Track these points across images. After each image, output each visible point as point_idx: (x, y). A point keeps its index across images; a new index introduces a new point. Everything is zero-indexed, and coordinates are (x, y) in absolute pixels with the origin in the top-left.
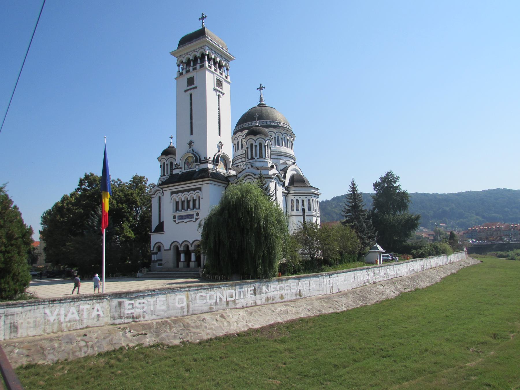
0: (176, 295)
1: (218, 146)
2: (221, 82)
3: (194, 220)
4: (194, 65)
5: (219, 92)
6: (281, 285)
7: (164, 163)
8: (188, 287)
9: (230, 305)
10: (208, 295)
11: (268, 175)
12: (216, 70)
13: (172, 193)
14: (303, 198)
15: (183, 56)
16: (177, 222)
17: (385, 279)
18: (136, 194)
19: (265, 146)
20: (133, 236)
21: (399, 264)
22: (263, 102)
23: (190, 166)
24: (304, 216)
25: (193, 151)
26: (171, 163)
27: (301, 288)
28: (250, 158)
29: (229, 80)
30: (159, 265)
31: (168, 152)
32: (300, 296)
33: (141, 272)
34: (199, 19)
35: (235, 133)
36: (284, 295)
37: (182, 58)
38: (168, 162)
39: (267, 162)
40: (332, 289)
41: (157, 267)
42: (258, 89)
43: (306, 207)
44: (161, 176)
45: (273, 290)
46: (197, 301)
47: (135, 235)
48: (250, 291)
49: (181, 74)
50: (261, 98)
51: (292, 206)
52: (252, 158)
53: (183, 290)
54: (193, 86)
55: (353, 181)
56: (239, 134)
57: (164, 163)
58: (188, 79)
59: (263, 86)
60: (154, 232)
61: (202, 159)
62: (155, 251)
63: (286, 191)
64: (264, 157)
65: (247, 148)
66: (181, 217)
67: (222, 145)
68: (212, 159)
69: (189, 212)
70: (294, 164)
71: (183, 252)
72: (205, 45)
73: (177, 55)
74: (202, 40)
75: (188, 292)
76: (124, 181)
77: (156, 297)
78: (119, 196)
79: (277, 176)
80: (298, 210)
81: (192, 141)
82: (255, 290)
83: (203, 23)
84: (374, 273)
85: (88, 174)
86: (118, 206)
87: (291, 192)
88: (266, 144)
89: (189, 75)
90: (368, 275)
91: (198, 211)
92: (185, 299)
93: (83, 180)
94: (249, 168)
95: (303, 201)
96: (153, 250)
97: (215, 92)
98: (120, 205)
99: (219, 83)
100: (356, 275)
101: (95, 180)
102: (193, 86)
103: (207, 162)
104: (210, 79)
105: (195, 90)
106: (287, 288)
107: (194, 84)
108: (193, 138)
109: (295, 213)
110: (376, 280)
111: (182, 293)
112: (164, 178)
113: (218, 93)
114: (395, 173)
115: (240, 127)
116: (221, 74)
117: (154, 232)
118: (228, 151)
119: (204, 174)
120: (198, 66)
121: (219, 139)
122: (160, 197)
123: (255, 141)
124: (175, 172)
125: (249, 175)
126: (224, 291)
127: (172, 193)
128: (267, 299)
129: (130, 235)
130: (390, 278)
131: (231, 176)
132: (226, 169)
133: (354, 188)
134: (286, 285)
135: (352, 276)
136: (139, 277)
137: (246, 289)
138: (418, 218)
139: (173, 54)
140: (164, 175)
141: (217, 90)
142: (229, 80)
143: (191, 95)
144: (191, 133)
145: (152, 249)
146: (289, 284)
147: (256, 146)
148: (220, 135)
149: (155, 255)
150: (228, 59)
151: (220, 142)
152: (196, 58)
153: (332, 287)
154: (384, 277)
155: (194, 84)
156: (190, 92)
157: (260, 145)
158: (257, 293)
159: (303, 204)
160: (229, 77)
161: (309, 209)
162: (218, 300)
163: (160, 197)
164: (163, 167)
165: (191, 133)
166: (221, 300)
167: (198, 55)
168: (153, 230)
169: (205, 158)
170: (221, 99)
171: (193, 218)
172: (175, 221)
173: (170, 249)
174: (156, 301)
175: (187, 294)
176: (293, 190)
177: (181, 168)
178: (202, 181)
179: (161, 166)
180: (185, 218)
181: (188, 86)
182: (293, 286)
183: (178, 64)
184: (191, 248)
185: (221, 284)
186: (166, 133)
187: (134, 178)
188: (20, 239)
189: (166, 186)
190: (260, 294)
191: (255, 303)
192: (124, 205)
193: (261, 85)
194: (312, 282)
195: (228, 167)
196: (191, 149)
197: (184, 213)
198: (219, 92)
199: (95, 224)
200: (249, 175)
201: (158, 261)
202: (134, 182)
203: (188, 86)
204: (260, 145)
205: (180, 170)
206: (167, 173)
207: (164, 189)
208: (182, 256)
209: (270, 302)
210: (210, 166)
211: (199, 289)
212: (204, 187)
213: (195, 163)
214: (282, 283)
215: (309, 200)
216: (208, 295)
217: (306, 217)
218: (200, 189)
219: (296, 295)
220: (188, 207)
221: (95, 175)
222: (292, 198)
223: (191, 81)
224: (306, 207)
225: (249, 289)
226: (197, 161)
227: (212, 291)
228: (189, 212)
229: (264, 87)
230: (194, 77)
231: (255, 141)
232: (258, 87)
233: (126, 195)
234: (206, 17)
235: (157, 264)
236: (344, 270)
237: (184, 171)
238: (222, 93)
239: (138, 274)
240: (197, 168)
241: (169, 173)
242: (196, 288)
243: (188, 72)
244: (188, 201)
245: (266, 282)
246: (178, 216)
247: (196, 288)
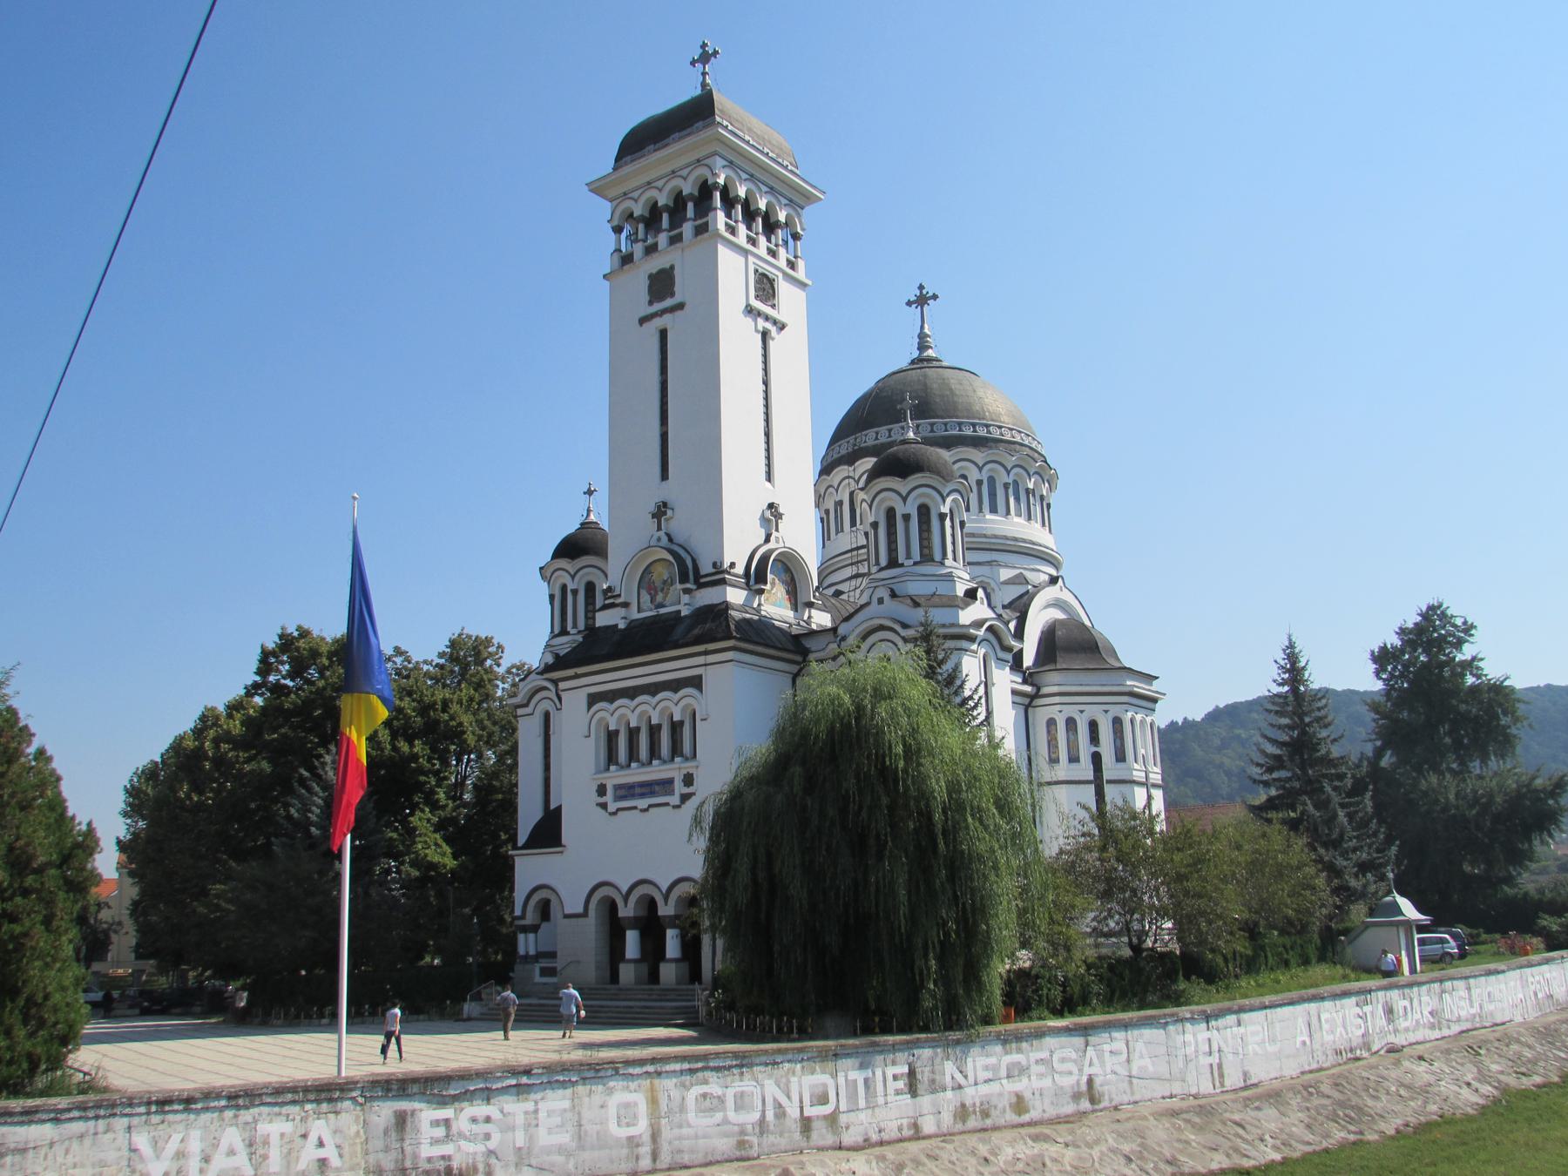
0: (611, 1091)
1: (765, 521)
2: (771, 282)
3: (675, 800)
4: (673, 226)
5: (767, 318)
6: (1015, 1057)
7: (564, 587)
8: (653, 1060)
9: (814, 1135)
10: (730, 1092)
11: (957, 625)
13: (593, 699)
15: (635, 195)
16: (612, 807)
17: (1437, 1034)
18: (460, 702)
19: (942, 517)
20: (450, 863)
21: (1489, 973)
22: (930, 353)
23: (659, 598)
24: (1098, 783)
25: (670, 540)
26: (590, 588)
27: (1092, 1071)
28: (883, 562)
29: (801, 274)
30: (547, 972)
31: (579, 546)
32: (1093, 1100)
33: (478, 998)
34: (693, 63)
35: (826, 469)
36: (1027, 1095)
37: (628, 204)
38: (578, 584)
39: (950, 575)
40: (1221, 1076)
41: (538, 979)
42: (909, 303)
44: (554, 636)
45: (983, 1075)
46: (691, 1116)
47: (455, 856)
48: (895, 1078)
49: (627, 259)
50: (922, 337)
51: (1052, 743)
52: (893, 563)
53: (637, 1070)
54: (668, 303)
55: (1291, 646)
56: (842, 471)
57: (564, 588)
58: (651, 276)
59: (930, 290)
60: (526, 846)
61: (706, 568)
62: (528, 921)
63: (1028, 689)
64: (938, 557)
65: (875, 525)
66: (627, 791)
67: (778, 516)
68: (739, 569)
69: (657, 771)
70: (1053, 580)
71: (635, 923)
72: (715, 154)
73: (613, 193)
74: (704, 135)
75: (657, 1081)
76: (416, 657)
77: (533, 1096)
78: (400, 710)
79: (990, 629)
80: (1074, 759)
81: (665, 504)
82: (912, 1074)
83: (704, 74)
84: (1389, 1011)
85: (292, 630)
86: (395, 749)
87: (1045, 690)
88: (945, 509)
89: (656, 263)
90: (1363, 1017)
91: (688, 767)
92: (643, 1108)
93: (273, 653)
94: (881, 601)
95: (1093, 726)
96: (523, 917)
97: (749, 321)
98: (404, 747)
99: (765, 287)
100: (1314, 1021)
101: (315, 654)
102: (668, 303)
103: (723, 582)
104: (733, 273)
105: (679, 313)
106: (1041, 1068)
107: (672, 295)
108: (670, 491)
109: (1063, 770)
110: (1399, 1040)
111: (633, 1085)
112: (565, 644)
113: (761, 324)
114: (1458, 610)
115: (844, 448)
116: (773, 253)
117: (526, 846)
118: (802, 536)
119: (712, 626)
120: (687, 229)
121: (768, 494)
122: (547, 716)
123: (905, 499)
124: (603, 619)
125: (882, 628)
126: (794, 1080)
127: (593, 699)
128: (962, 1112)
129: (437, 859)
130: (1456, 1029)
131: (813, 633)
132: (795, 608)
133: (1294, 671)
134: (1035, 1056)
135: (1301, 1023)
136: (469, 1019)
137: (879, 1072)
138: (1558, 787)
139: (598, 188)
140: (564, 632)
141: (759, 314)
142: (801, 274)
143: (663, 334)
144: (664, 475)
145: (518, 912)
146: (1044, 1055)
147: (907, 517)
148: (769, 478)
149: (531, 936)
150: (799, 199)
151: (771, 506)
152: (679, 201)
153: (1220, 1066)
154: (1432, 1027)
155: (672, 295)
156: (658, 323)
157: (924, 511)
158: (921, 1088)
159: (1094, 738)
160: (801, 264)
161: (1120, 757)
162: (770, 1115)
163: (547, 716)
164: (560, 600)
165: (664, 475)
166: (781, 1113)
167: (688, 188)
168: (521, 840)
169: (715, 565)
170: (772, 344)
171: (672, 793)
172: (604, 806)
173: (585, 914)
174: (536, 1111)
175: (652, 1089)
176: (1053, 682)
177: (626, 605)
178: (706, 653)
179: (552, 597)
180: (642, 795)
181: (651, 303)
182: (1063, 1060)
183: (615, 223)
184: (666, 910)
185: (779, 1051)
186: (571, 473)
187: (453, 644)
188: (53, 872)
189: (571, 672)
190: (934, 1091)
191: (915, 1126)
192: (418, 746)
193: (921, 287)
194: (1139, 1046)
195: (802, 599)
196: (661, 533)
197: (637, 774)
198: (767, 318)
199: (313, 818)
200: (882, 628)
201: (540, 956)
202: (453, 658)
203: (651, 303)
204: (924, 511)
205: (621, 611)
206: (575, 626)
207: (562, 685)
208: (632, 937)
209: (972, 1123)
210: (735, 596)
211: (697, 1067)
212: (711, 677)
213: (679, 586)
214: (1019, 1051)
215: (1117, 722)
216: (730, 1092)
218: (696, 683)
219: (1076, 1096)
220: (654, 752)
221: (315, 633)
222: (1052, 712)
223: (661, 284)
225: (891, 1071)
226: (684, 578)
227: (747, 1076)
228: (657, 771)
229: (935, 297)
231: (905, 499)
232: (913, 294)
233: (425, 709)
234: (716, 53)
235: (537, 967)
236: (1267, 1000)
237: (636, 616)
238: (775, 322)
239: (469, 1008)
240: (683, 603)
241: (581, 626)
242: (686, 1066)
243: (651, 250)
244: (654, 731)
245: (958, 1042)
246: (617, 787)
247: (686, 1066)
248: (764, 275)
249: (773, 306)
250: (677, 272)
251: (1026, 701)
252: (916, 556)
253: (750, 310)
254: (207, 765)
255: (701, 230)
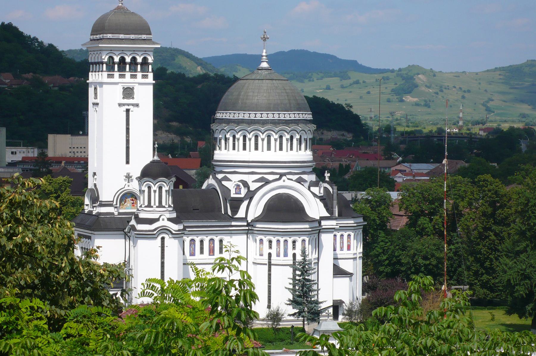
5: (128, 105)
14: (271, 238)
24: (270, 265)
43: (274, 252)
80: (261, 255)
99: (128, 92)
141: (124, 105)
148: (128, 162)
161: (278, 255)
198: (128, 105)
217: (272, 267)
224: (274, 252)
238: (133, 105)
249: (133, 98)
251: (247, 231)
252: (146, 204)
253: (120, 105)
254: (264, 65)
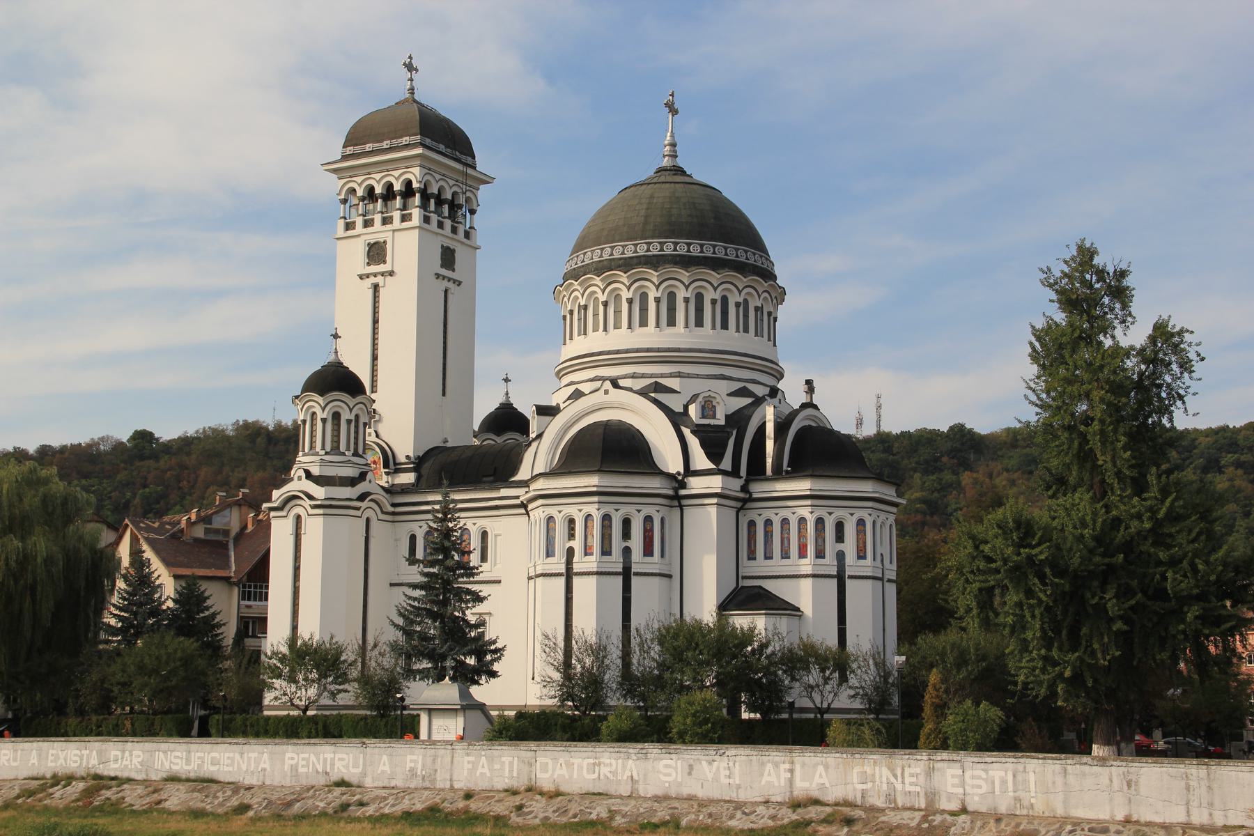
12: (440, 225)
99: (448, 258)
107: (385, 262)
113: (445, 284)
141: (444, 278)
155: (385, 262)
156: (372, 280)
170: (450, 296)
203: (368, 264)
230: (385, 242)
238: (455, 281)
248: (448, 248)
249: (454, 270)
250: (389, 247)
253: (438, 276)
255: (405, 218)
